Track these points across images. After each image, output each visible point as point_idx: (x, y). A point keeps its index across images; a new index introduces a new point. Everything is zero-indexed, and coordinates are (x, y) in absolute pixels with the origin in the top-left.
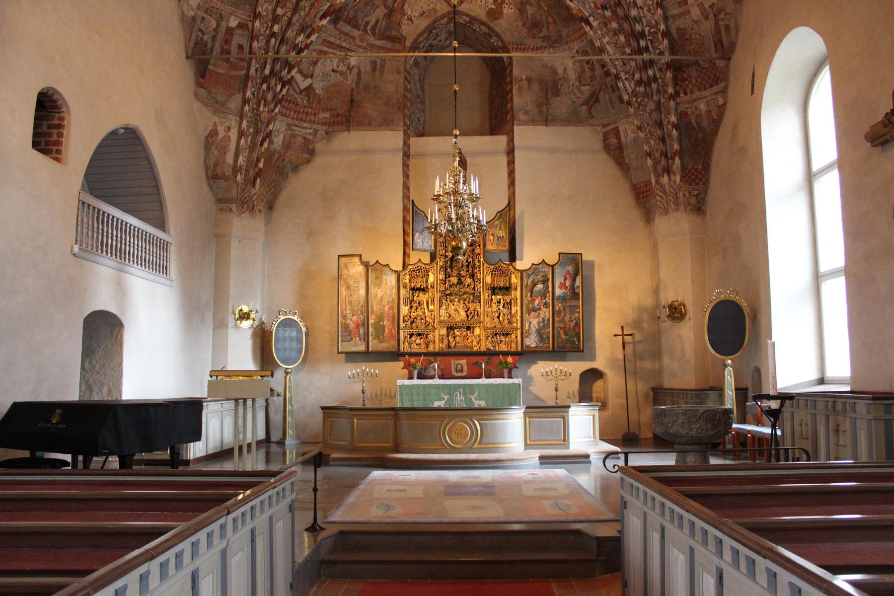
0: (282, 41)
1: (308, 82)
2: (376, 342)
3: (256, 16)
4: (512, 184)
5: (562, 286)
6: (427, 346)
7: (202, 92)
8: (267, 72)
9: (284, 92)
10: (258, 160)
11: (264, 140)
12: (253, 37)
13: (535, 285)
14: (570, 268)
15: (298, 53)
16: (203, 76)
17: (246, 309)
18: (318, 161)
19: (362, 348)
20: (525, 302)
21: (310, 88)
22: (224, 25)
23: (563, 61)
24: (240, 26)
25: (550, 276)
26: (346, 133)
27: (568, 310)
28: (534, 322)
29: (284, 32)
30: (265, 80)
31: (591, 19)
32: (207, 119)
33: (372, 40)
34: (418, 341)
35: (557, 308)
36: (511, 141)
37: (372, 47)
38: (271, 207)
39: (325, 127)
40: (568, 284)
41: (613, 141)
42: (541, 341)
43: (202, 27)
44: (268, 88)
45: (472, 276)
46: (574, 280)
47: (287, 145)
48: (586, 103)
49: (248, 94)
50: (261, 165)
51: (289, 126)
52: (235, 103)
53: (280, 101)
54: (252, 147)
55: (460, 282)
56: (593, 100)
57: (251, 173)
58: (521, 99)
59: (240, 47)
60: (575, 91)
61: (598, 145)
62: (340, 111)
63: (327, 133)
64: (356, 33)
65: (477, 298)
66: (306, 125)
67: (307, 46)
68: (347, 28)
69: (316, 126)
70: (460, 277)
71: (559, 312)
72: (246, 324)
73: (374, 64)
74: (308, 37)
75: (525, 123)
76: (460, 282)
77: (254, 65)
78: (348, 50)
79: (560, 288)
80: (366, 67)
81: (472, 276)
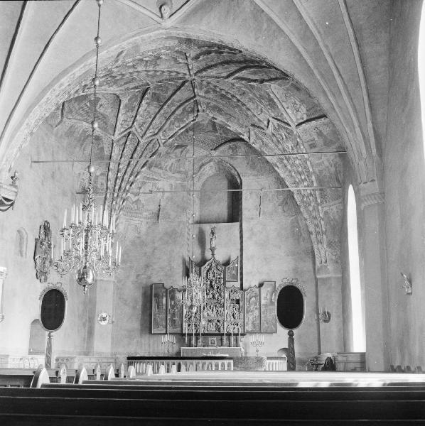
1: (137, 197)
5: (266, 298)
8: (116, 195)
9: (124, 204)
17: (104, 315)
19: (164, 332)
24: (102, 174)
27: (268, 311)
33: (170, 174)
35: (262, 310)
36: (241, 226)
37: (171, 177)
40: (268, 297)
46: (271, 296)
51: (127, 220)
59: (102, 184)
64: (160, 171)
69: (142, 219)
72: (103, 323)
74: (136, 176)
78: (157, 180)
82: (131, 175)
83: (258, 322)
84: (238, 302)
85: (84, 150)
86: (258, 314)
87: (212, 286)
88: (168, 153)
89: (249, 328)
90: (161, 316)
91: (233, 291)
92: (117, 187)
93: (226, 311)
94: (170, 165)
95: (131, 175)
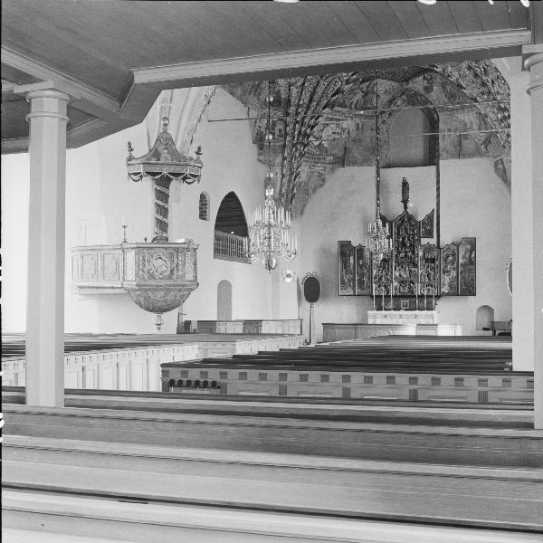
0: (302, 125)
2: (360, 290)
3: (288, 114)
7: (262, 158)
10: (293, 189)
11: (296, 177)
12: (286, 125)
13: (448, 257)
14: (469, 247)
15: (312, 129)
16: (261, 149)
18: (327, 185)
19: (352, 293)
21: (320, 145)
22: (271, 121)
23: (469, 117)
28: (446, 279)
29: (303, 119)
30: (294, 146)
31: (478, 98)
32: (263, 171)
38: (302, 213)
41: (500, 166)
43: (260, 125)
44: (296, 149)
46: (471, 253)
47: (309, 178)
49: (286, 154)
50: (295, 191)
52: (279, 159)
53: (303, 155)
54: (289, 181)
57: (290, 196)
58: (444, 143)
59: (280, 130)
67: (316, 124)
68: (340, 109)
72: (288, 280)
73: (358, 124)
74: (317, 119)
77: (288, 138)
80: (352, 128)
81: (413, 253)
82: (312, 117)
84: (433, 261)
85: (259, 95)
86: (455, 275)
87: (403, 244)
88: (352, 91)
91: (428, 248)
92: (296, 133)
93: (420, 272)
94: (355, 102)
95: (312, 117)
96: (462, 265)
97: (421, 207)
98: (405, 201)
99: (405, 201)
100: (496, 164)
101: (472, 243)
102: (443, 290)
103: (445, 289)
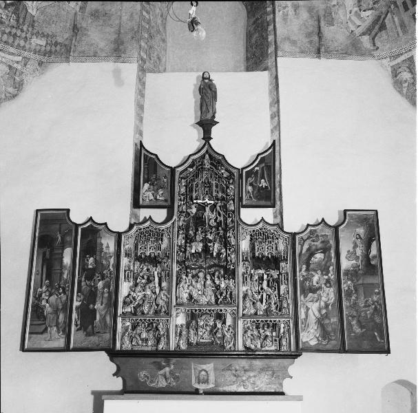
2: (81, 334)
4: (276, 115)
6: (158, 341)
13: (311, 254)
20: (299, 278)
25: (332, 242)
26: (65, 64)
27: (361, 291)
28: (311, 309)
34: (144, 335)
35: (344, 287)
39: (38, 57)
40: (359, 252)
41: (406, 75)
42: (324, 337)
45: (226, 244)
46: (368, 247)
48: (368, 31)
55: (206, 249)
56: (377, 27)
60: (354, 18)
61: (386, 81)
62: (60, 40)
63: (41, 63)
65: (231, 274)
66: (12, 50)
69: (26, 54)
70: (205, 241)
71: (349, 294)
75: (293, 55)
76: (206, 249)
79: (348, 258)
81: (226, 244)
83: (334, 320)
89: (309, 336)
90: (53, 298)
91: (260, 234)
96: (347, 272)
97: (238, 146)
98: (206, 125)
99: (206, 125)
100: (395, 73)
101: (369, 225)
102: (304, 337)
103: (309, 336)
